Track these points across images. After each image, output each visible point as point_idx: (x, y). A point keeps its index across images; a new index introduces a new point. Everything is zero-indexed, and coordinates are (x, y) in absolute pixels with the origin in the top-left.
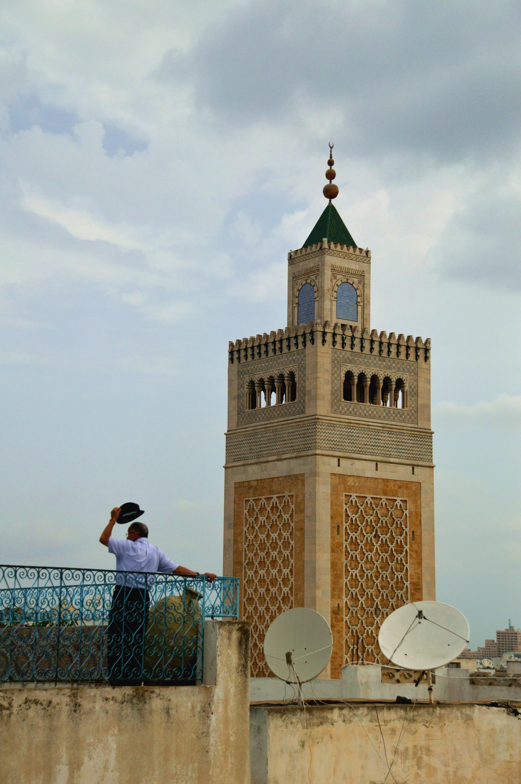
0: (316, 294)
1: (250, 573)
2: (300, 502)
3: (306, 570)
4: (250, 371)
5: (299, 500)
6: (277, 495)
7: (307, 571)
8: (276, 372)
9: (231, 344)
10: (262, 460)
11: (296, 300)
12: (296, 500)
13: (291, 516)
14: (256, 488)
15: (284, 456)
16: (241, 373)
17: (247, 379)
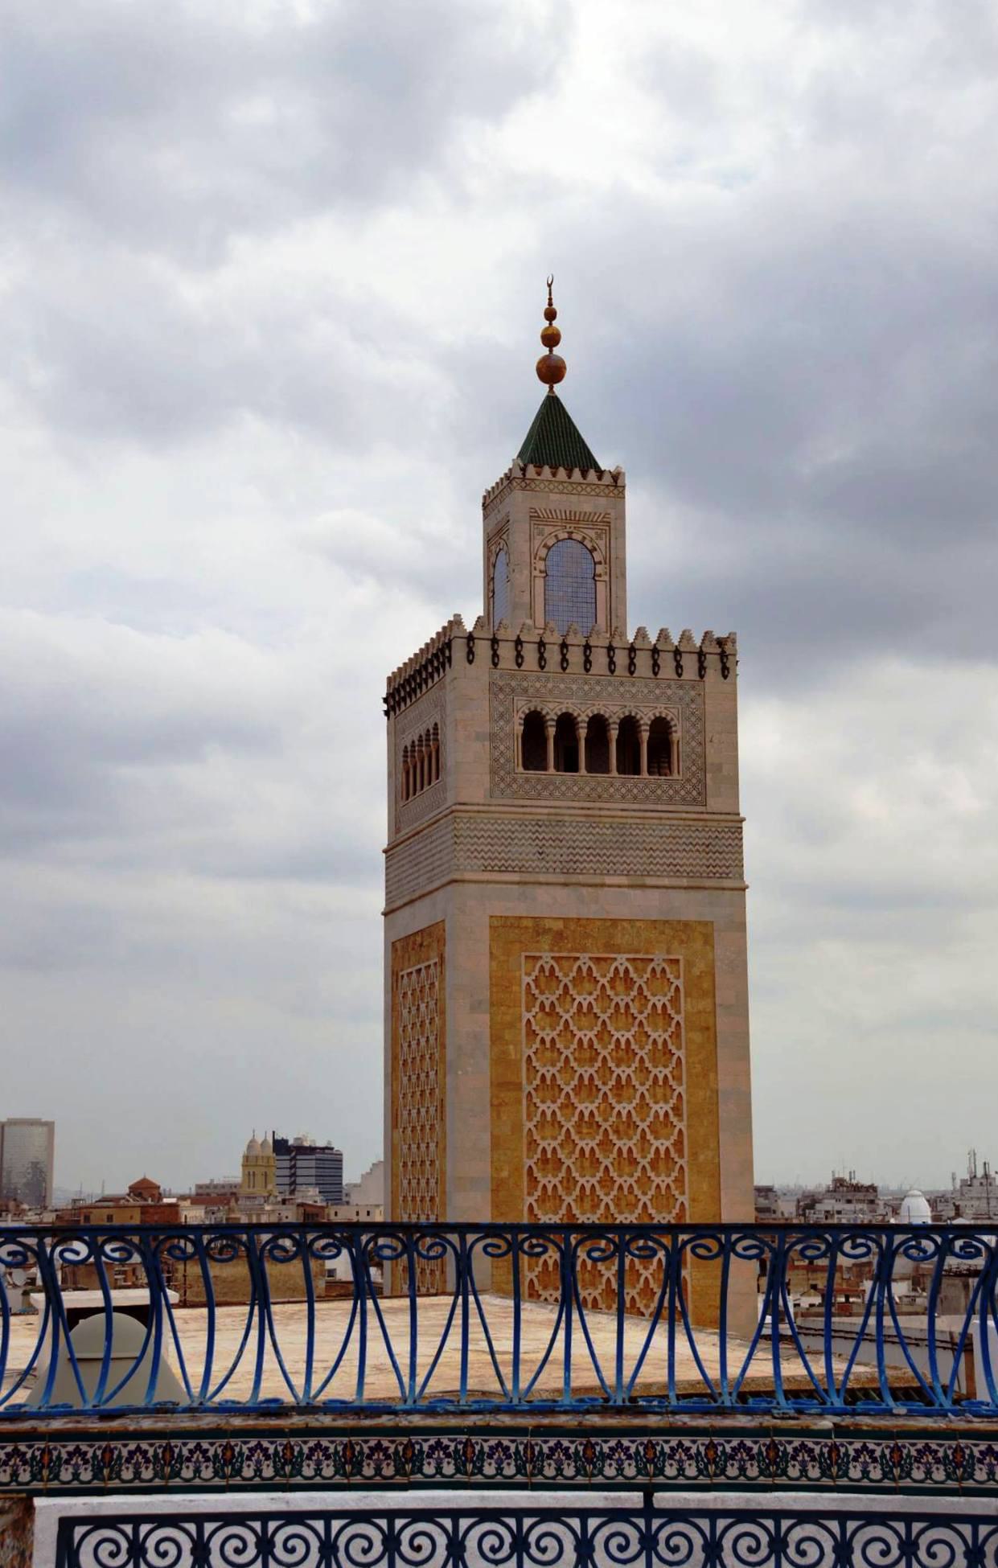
0: (600, 569)
1: (549, 1107)
2: (699, 977)
3: (722, 1107)
4: (531, 690)
5: (696, 971)
6: (631, 956)
7: (726, 1111)
8: (616, 709)
9: (456, 622)
10: (581, 878)
11: (541, 565)
12: (688, 971)
13: (675, 1000)
14: (559, 936)
15: (649, 881)
16: (501, 689)
17: (523, 707)
